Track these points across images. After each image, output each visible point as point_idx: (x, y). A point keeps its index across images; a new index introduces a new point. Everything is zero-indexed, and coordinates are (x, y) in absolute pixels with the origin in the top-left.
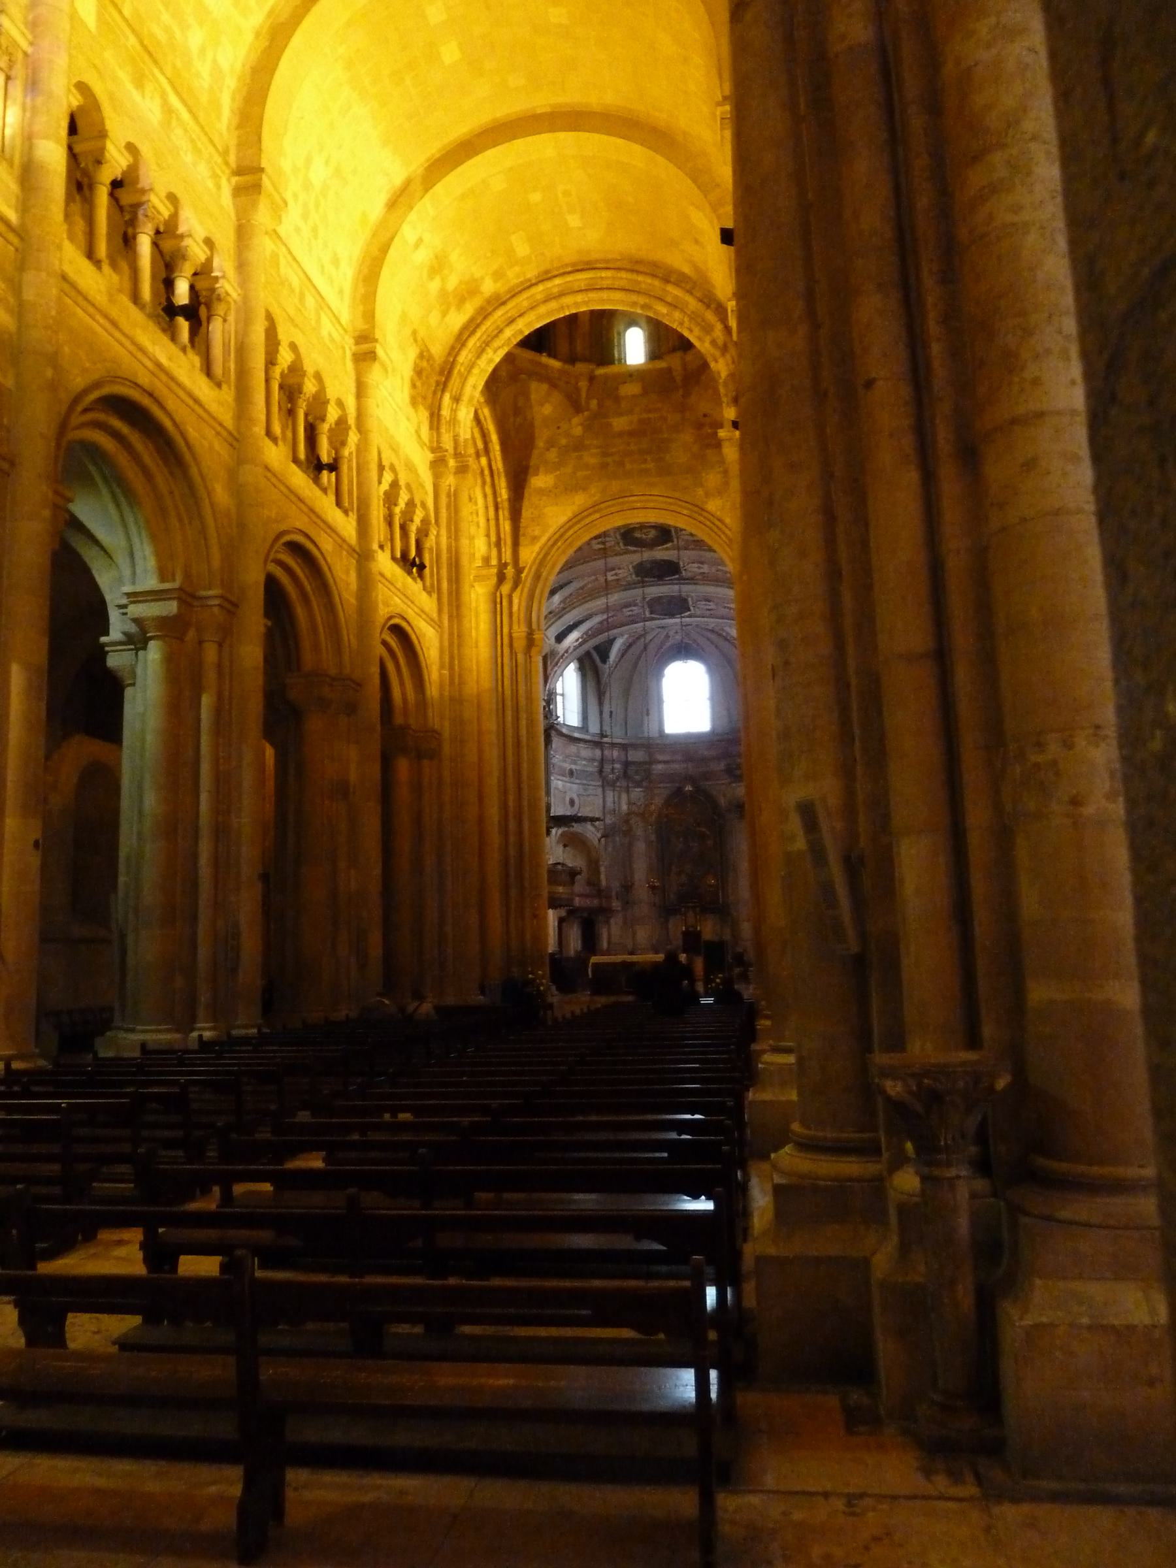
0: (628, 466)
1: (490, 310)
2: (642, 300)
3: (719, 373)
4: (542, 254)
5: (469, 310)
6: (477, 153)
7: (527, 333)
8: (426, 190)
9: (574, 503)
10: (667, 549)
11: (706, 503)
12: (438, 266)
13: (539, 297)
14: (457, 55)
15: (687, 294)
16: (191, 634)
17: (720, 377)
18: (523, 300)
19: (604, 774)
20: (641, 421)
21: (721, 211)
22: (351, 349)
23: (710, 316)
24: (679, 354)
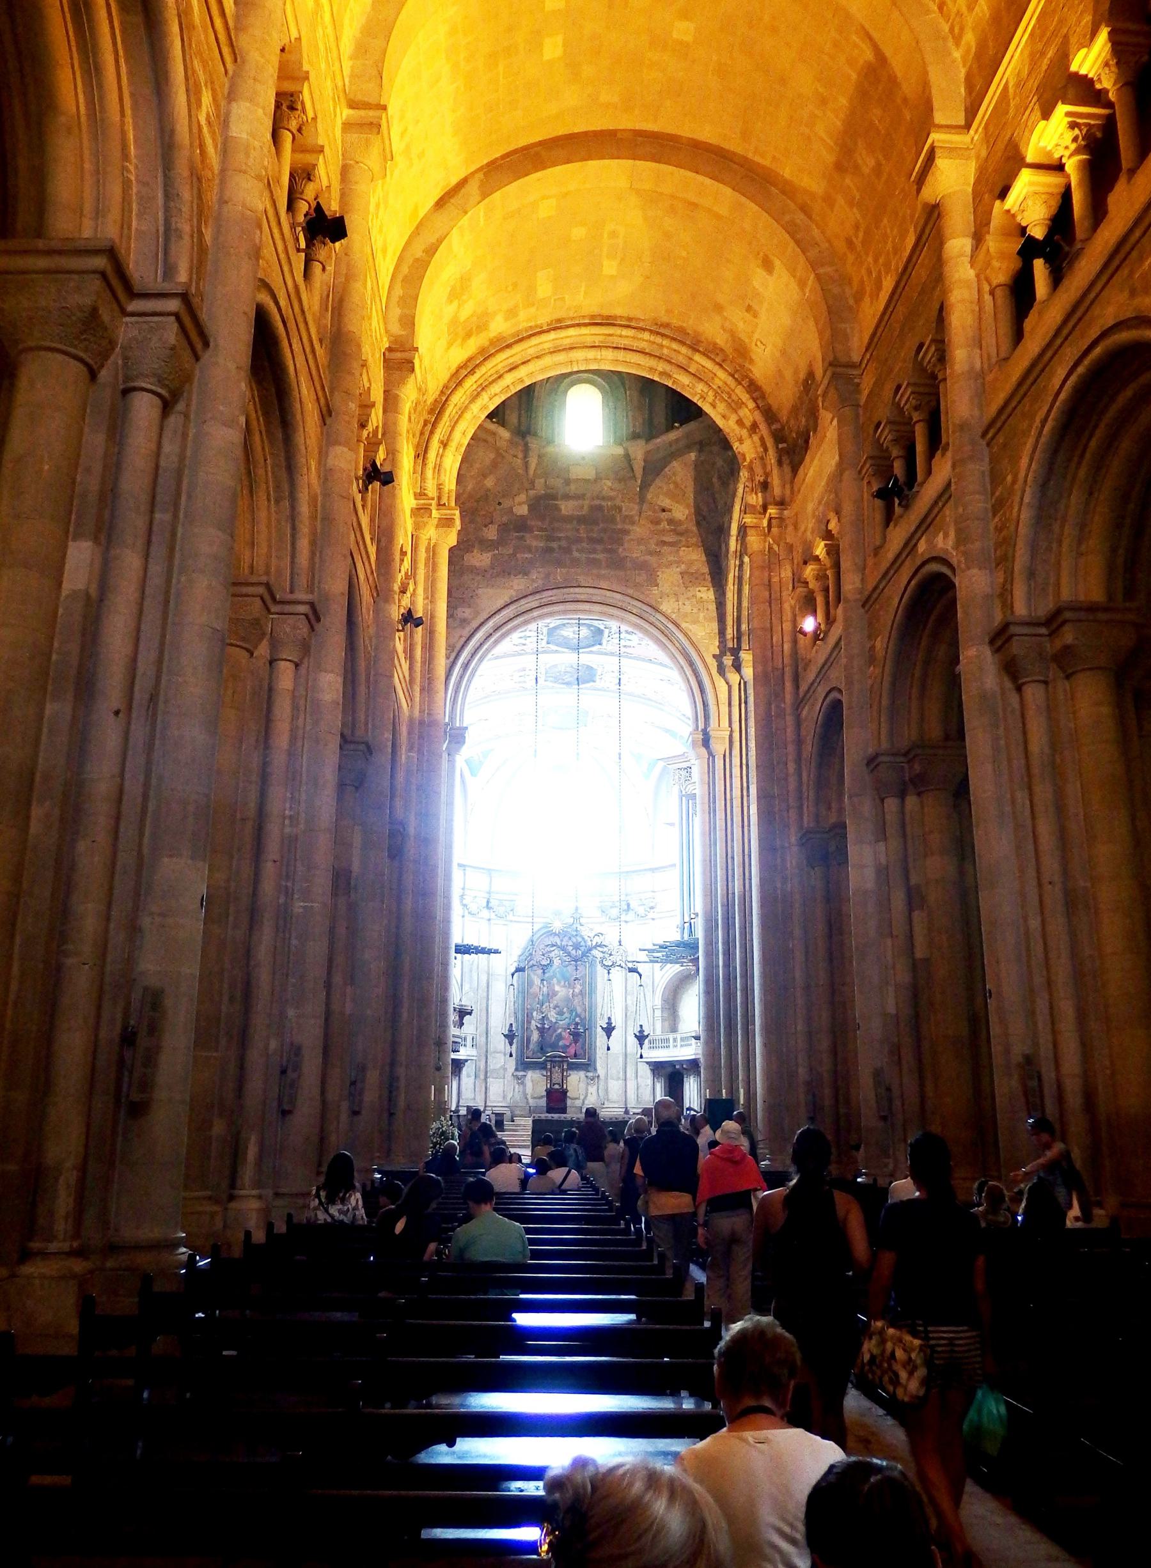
0: (576, 554)
2: (661, 366)
3: (744, 455)
4: (563, 299)
5: (472, 347)
8: (485, 195)
10: (591, 652)
12: (458, 291)
13: (546, 346)
14: (559, 52)
15: (717, 367)
16: (263, 650)
17: (745, 459)
19: (465, 902)
21: (821, 271)
22: (384, 354)
23: (742, 394)
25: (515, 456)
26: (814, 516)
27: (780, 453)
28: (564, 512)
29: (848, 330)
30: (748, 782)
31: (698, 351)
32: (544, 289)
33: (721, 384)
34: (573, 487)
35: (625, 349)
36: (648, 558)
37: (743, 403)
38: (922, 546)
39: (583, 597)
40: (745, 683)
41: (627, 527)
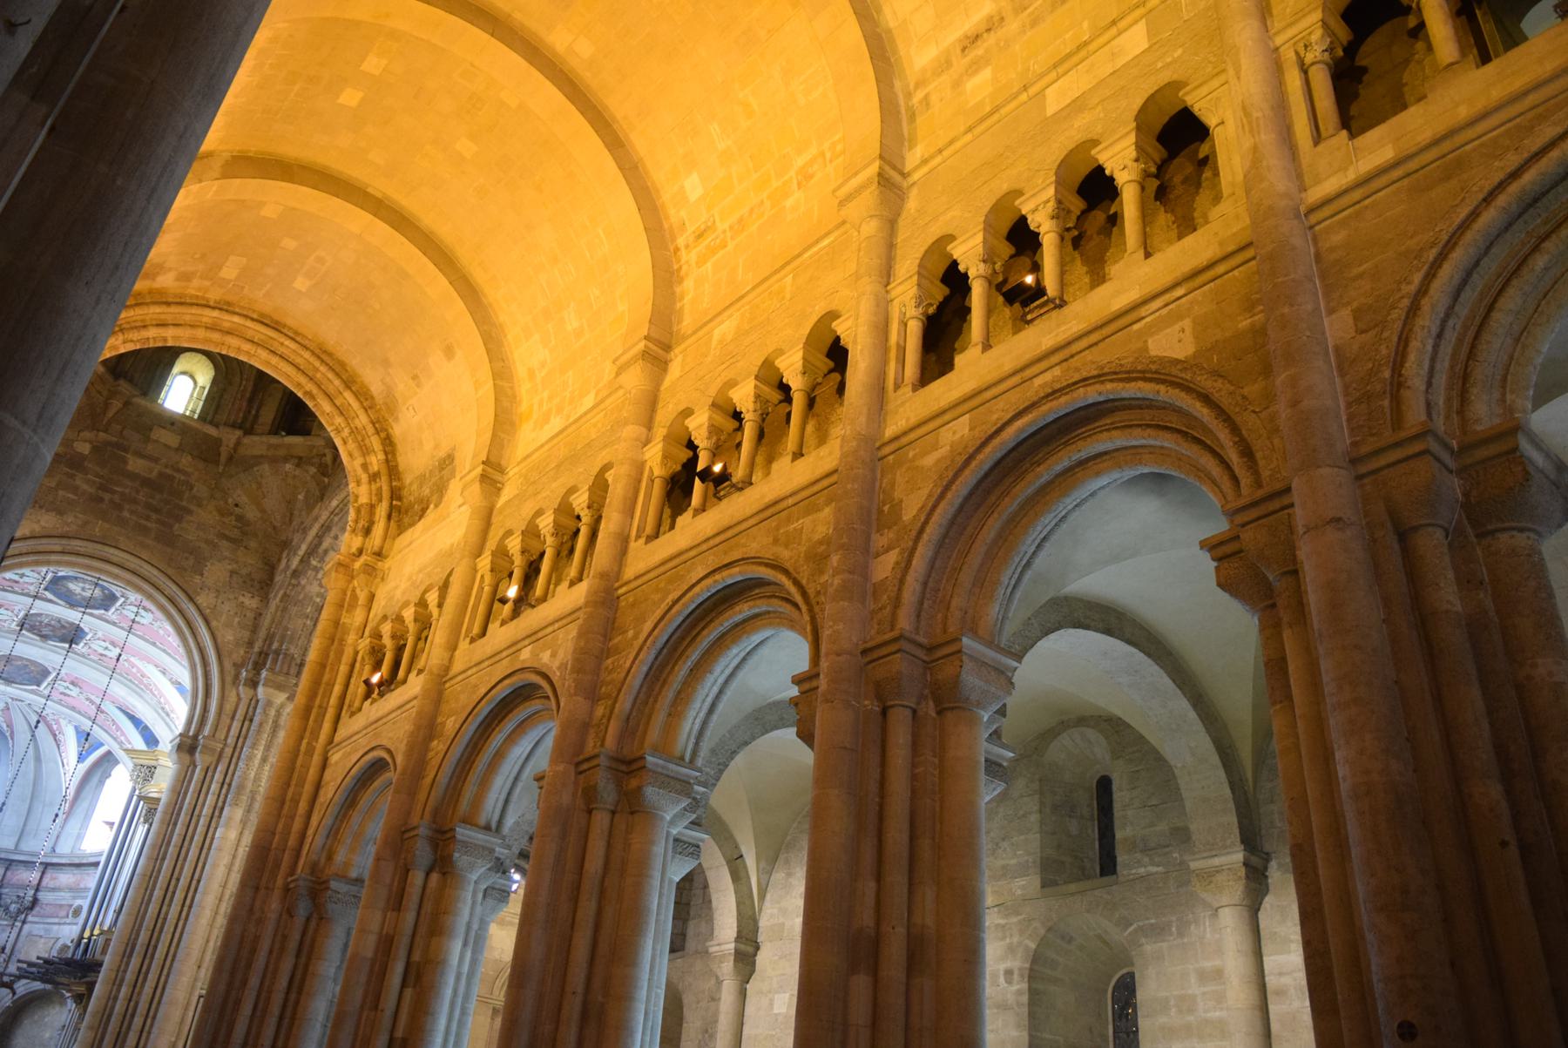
0: (126, 514)
1: (148, 301)
2: (310, 386)
3: (357, 497)
4: (243, 288)
6: (291, 180)
7: (170, 344)
9: (39, 521)
11: (199, 594)
13: (204, 320)
14: (354, 103)
17: (356, 501)
18: (188, 314)
20: (161, 474)
23: (375, 443)
24: (239, 433)
25: (99, 393)
26: (410, 578)
27: (391, 506)
28: (129, 468)
29: (506, 441)
30: (224, 802)
31: (351, 390)
32: (229, 272)
33: (360, 426)
34: (150, 447)
35: (281, 356)
36: (203, 545)
37: (374, 451)
38: (525, 654)
39: (115, 559)
40: (258, 701)
41: (192, 507)
